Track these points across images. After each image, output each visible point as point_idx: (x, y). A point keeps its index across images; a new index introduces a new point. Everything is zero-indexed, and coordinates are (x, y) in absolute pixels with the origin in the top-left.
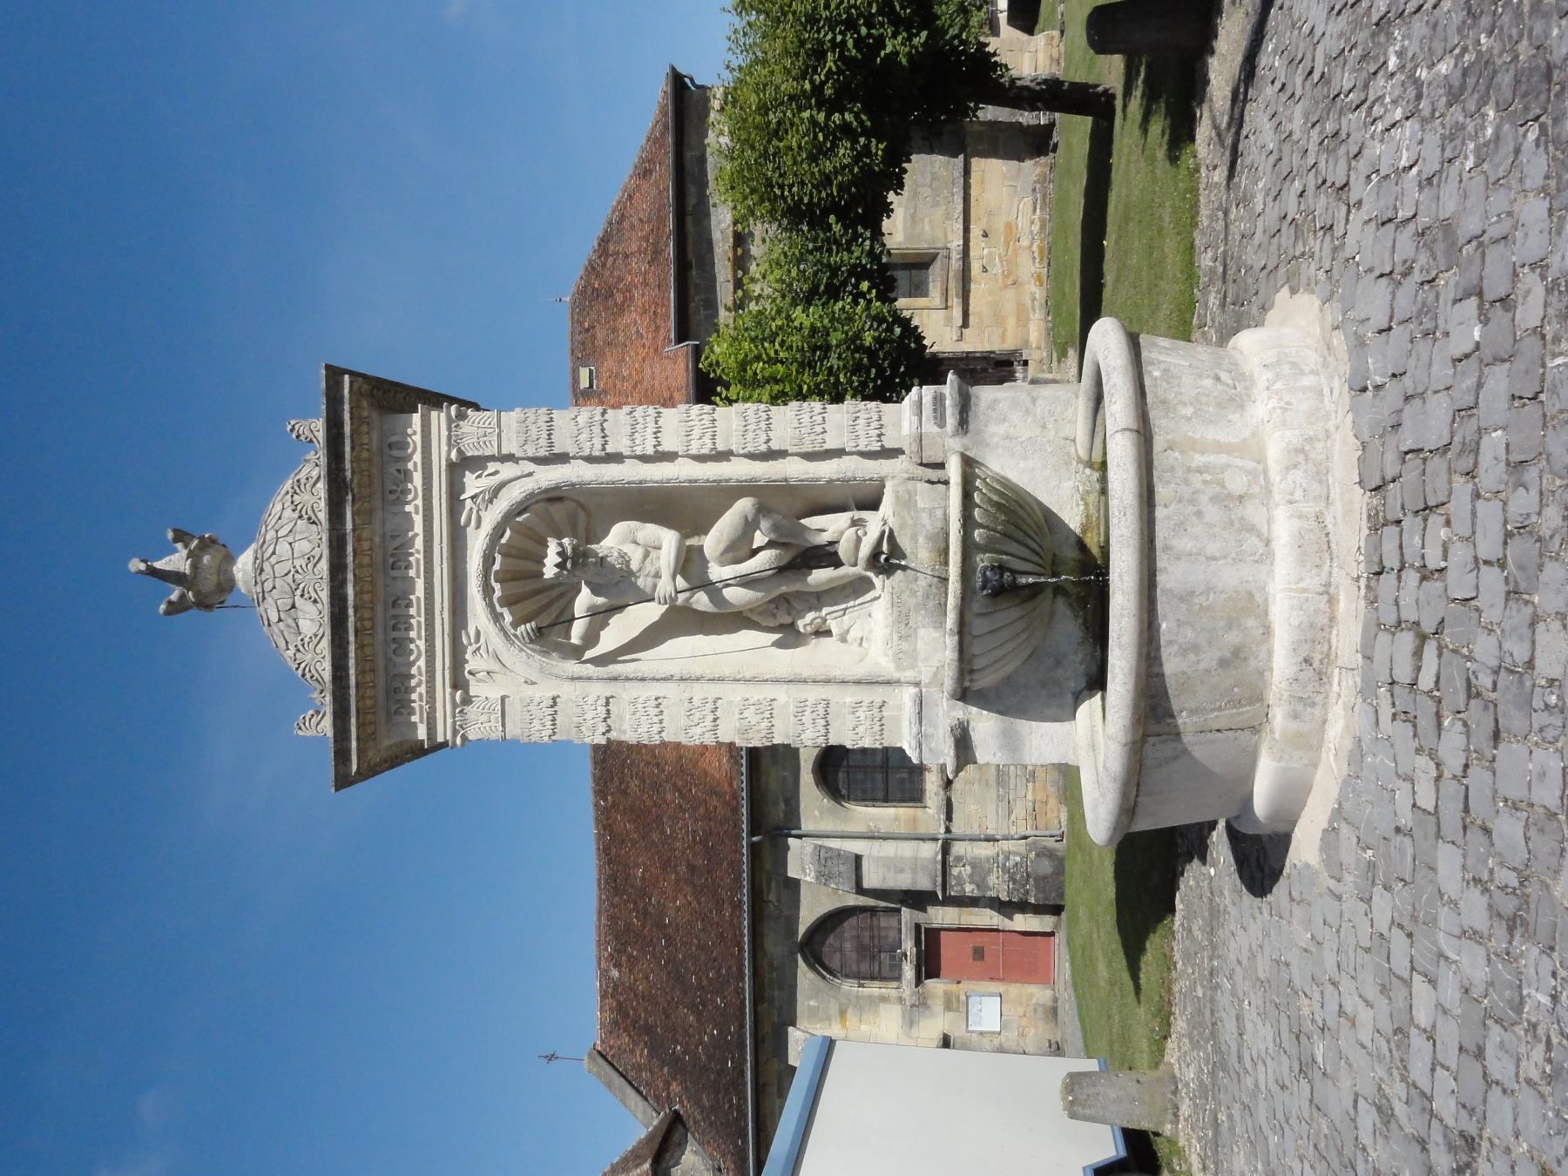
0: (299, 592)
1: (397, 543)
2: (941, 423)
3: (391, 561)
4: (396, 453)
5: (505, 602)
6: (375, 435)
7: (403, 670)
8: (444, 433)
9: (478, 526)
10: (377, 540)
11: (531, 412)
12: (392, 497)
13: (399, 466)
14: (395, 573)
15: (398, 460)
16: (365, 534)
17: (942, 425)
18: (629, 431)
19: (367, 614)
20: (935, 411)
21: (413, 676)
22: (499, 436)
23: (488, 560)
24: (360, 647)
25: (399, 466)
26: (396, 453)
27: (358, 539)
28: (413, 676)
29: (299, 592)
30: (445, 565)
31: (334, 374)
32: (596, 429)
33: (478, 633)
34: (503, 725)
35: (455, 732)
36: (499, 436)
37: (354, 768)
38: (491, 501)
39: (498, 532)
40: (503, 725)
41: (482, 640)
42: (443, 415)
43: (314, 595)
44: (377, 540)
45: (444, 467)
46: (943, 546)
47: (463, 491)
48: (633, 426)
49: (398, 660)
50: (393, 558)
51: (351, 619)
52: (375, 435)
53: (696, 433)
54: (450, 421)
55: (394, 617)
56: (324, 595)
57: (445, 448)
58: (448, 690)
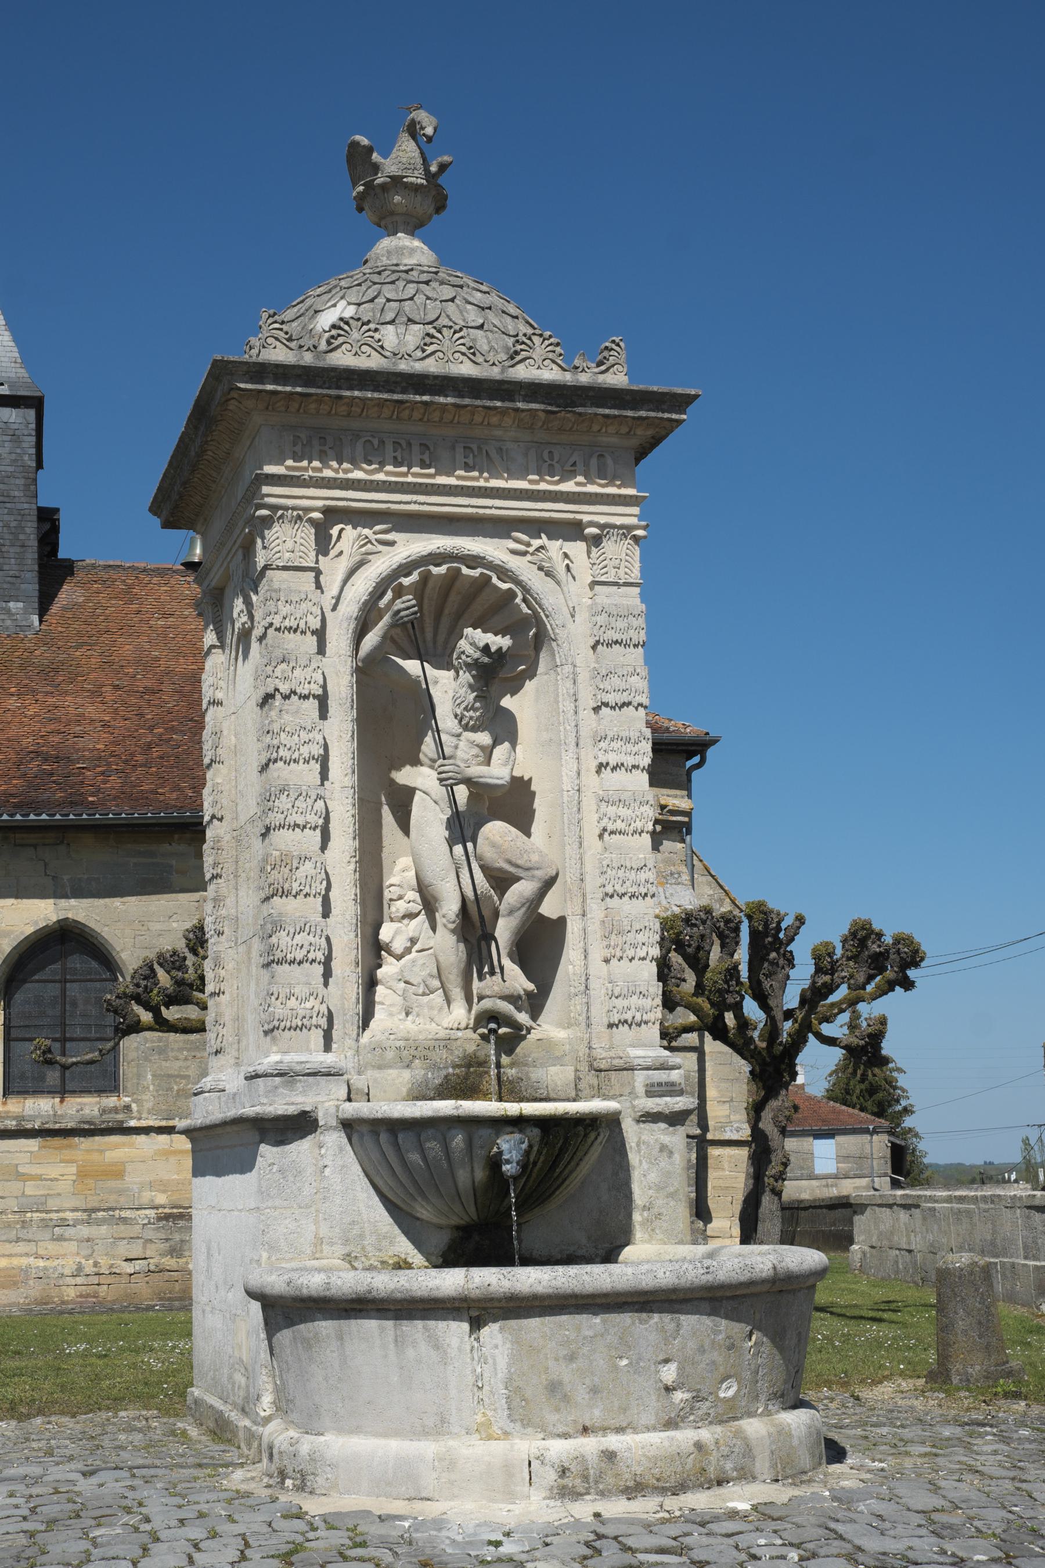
0: (433, 331)
1: (493, 454)
2: (652, 1091)
3: (474, 447)
4: (594, 461)
5: (511, 595)
6: (614, 440)
7: (347, 451)
8: (618, 521)
9: (514, 552)
10: (498, 433)
11: (641, 622)
12: (546, 456)
13: (580, 466)
14: (459, 450)
15: (587, 465)
16: (508, 421)
17: (649, 1094)
18: (624, 734)
19: (416, 415)
20: (660, 1084)
21: (340, 463)
22: (616, 584)
23: (474, 561)
24: (381, 404)
25: (580, 466)
26: (594, 461)
27: (503, 412)
28: (340, 463)
29: (433, 331)
30: (474, 510)
31: (682, 402)
32: (625, 697)
33: (391, 544)
34: (285, 568)
35: (274, 508)
36: (616, 584)
37: (242, 386)
38: (540, 569)
39: (504, 573)
40: (285, 568)
41: (380, 548)
42: (634, 521)
43: (430, 349)
44: (498, 433)
45: (578, 517)
46: (552, 1095)
47: (550, 538)
48: (628, 740)
49: (359, 446)
50: (478, 454)
51: (418, 398)
52: (614, 440)
53: (623, 812)
54: (629, 528)
55: (409, 444)
56: (431, 366)
57: (602, 520)
58: (320, 503)
